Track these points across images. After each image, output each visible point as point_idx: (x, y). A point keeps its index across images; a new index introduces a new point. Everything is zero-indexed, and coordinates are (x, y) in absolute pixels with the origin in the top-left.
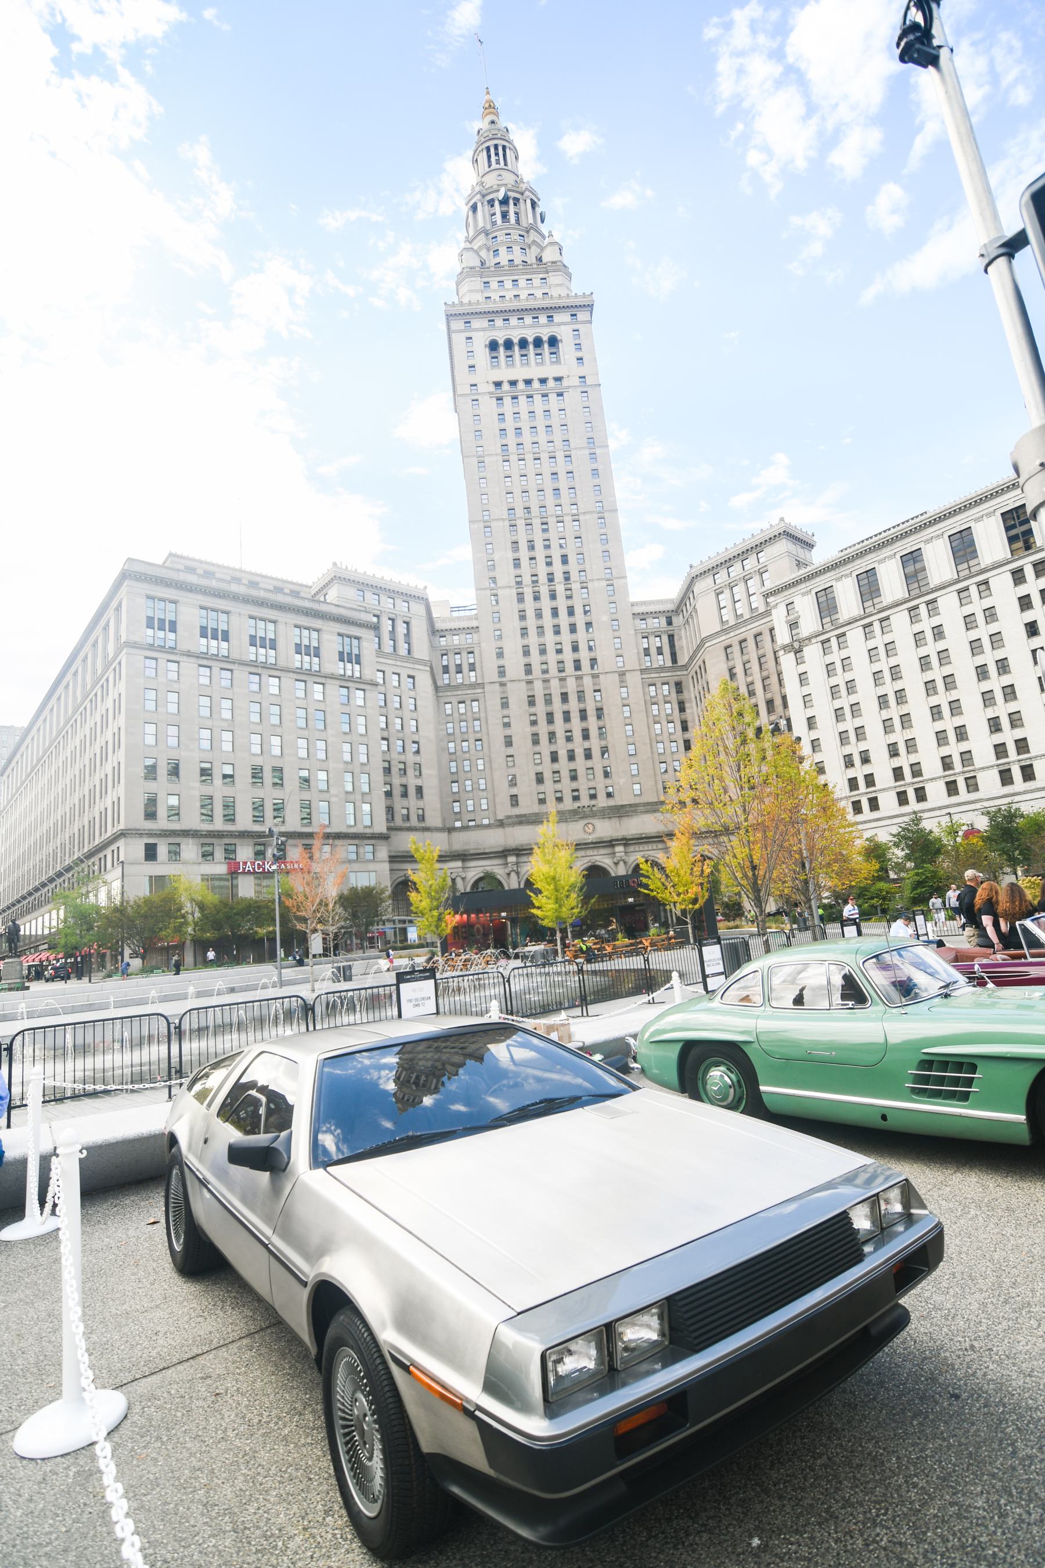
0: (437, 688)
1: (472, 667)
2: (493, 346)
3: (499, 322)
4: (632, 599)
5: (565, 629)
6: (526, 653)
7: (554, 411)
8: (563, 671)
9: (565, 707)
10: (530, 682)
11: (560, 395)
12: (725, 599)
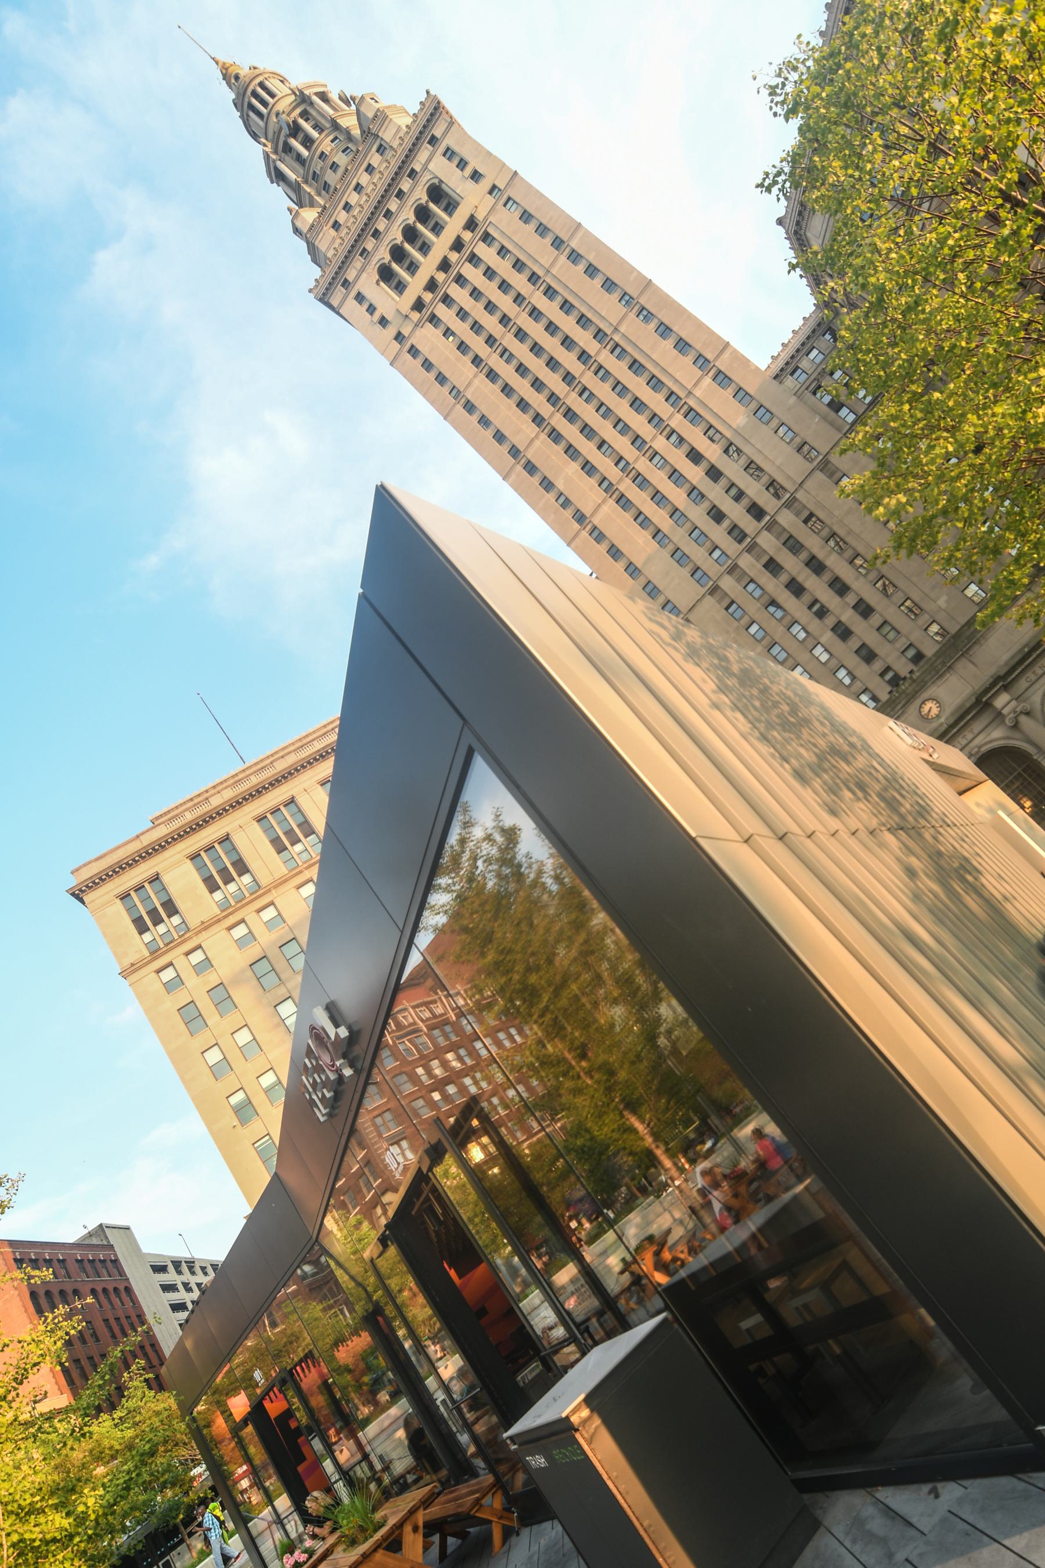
2: (386, 274)
3: (370, 244)
8: (745, 535)
9: (784, 578)
10: (714, 590)
11: (487, 238)
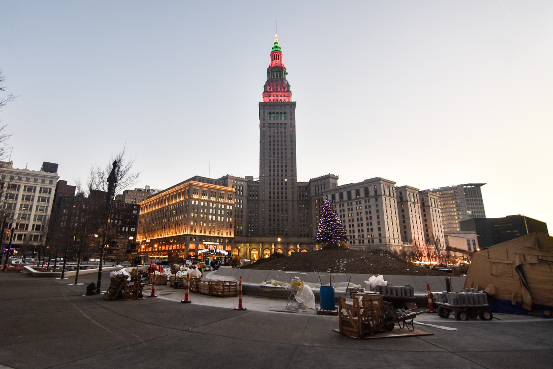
0: (248, 200)
1: (257, 196)
2: (270, 113)
3: (272, 108)
4: (298, 181)
5: (280, 188)
6: (270, 193)
7: (283, 132)
11: (285, 128)
12: (317, 188)
